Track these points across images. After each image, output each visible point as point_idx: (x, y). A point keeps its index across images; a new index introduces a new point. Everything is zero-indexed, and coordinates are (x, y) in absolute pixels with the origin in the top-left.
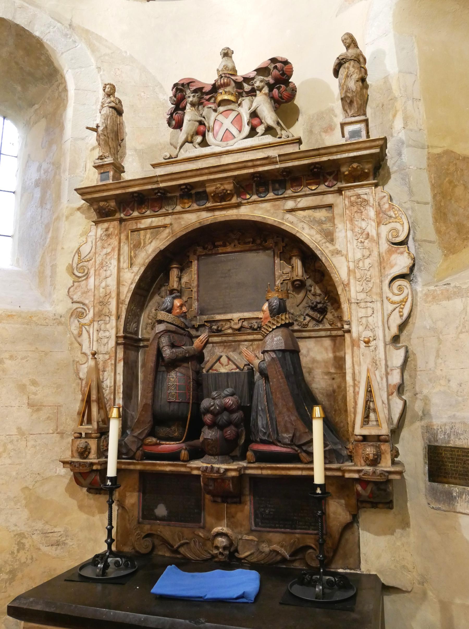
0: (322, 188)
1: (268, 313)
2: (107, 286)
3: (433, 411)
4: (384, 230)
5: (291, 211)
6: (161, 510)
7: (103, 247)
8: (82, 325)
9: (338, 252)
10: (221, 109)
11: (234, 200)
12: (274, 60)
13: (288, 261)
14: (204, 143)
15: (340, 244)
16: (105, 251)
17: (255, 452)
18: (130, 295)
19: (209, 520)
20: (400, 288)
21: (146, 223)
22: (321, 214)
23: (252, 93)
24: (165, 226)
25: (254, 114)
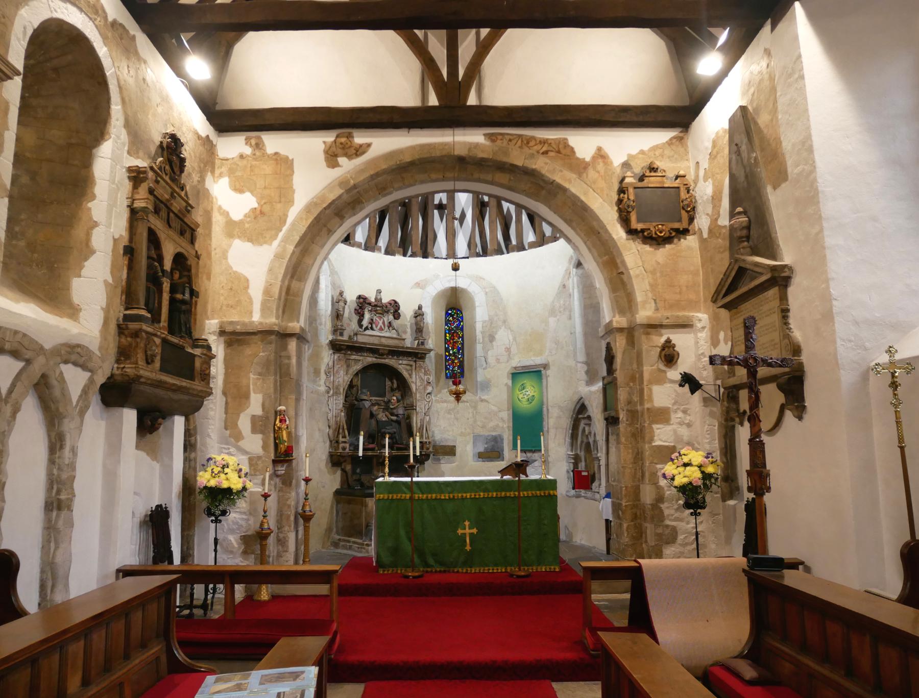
0: (410, 359)
1: (396, 401)
2: (339, 381)
3: (435, 435)
4: (426, 377)
5: (400, 364)
6: (358, 471)
7: (337, 364)
8: (329, 397)
9: (413, 382)
10: (377, 315)
11: (385, 356)
12: (395, 302)
13: (391, 380)
14: (372, 329)
15: (414, 380)
16: (338, 366)
17: (396, 447)
18: (347, 386)
19: (375, 473)
20: (429, 397)
21: (353, 357)
22: (408, 368)
23: (387, 312)
24: (360, 360)
25: (390, 323)
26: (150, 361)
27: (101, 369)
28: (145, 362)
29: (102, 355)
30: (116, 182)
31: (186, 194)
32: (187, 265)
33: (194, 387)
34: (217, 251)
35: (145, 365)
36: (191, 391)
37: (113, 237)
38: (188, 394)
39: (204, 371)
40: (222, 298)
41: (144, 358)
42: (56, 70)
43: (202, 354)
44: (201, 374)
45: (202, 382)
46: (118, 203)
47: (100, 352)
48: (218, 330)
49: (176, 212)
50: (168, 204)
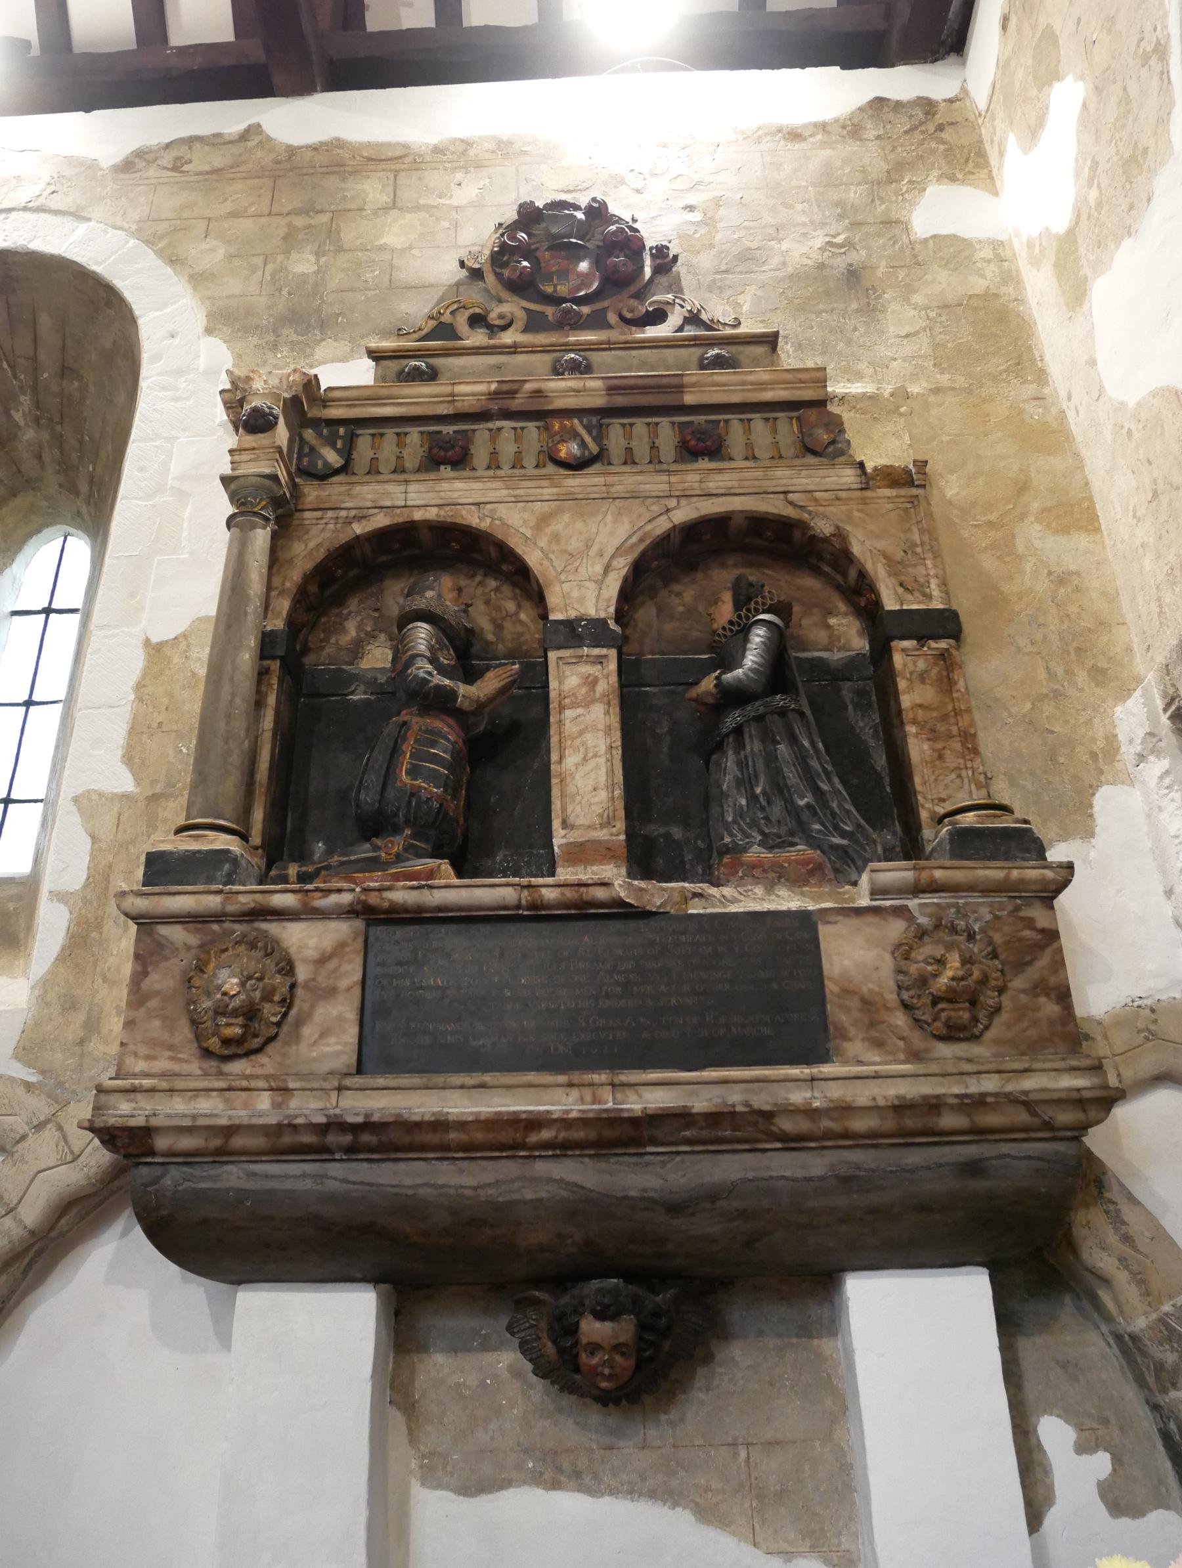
26: (214, 1043)
27: (50, 1133)
28: (189, 1051)
29: (43, 1072)
30: (170, 482)
31: (693, 319)
32: (825, 540)
33: (798, 1097)
34: (1075, 398)
35: (194, 1067)
36: (786, 1125)
37: (147, 643)
38: (792, 1142)
39: (923, 981)
40: (1148, 564)
41: (184, 1031)
42: (65, 371)
43: (875, 893)
44: (906, 1006)
45: (946, 1050)
46: (185, 534)
47: (28, 1064)
48: (1164, 719)
49: (600, 401)
50: (517, 404)
